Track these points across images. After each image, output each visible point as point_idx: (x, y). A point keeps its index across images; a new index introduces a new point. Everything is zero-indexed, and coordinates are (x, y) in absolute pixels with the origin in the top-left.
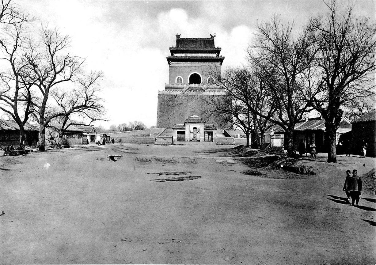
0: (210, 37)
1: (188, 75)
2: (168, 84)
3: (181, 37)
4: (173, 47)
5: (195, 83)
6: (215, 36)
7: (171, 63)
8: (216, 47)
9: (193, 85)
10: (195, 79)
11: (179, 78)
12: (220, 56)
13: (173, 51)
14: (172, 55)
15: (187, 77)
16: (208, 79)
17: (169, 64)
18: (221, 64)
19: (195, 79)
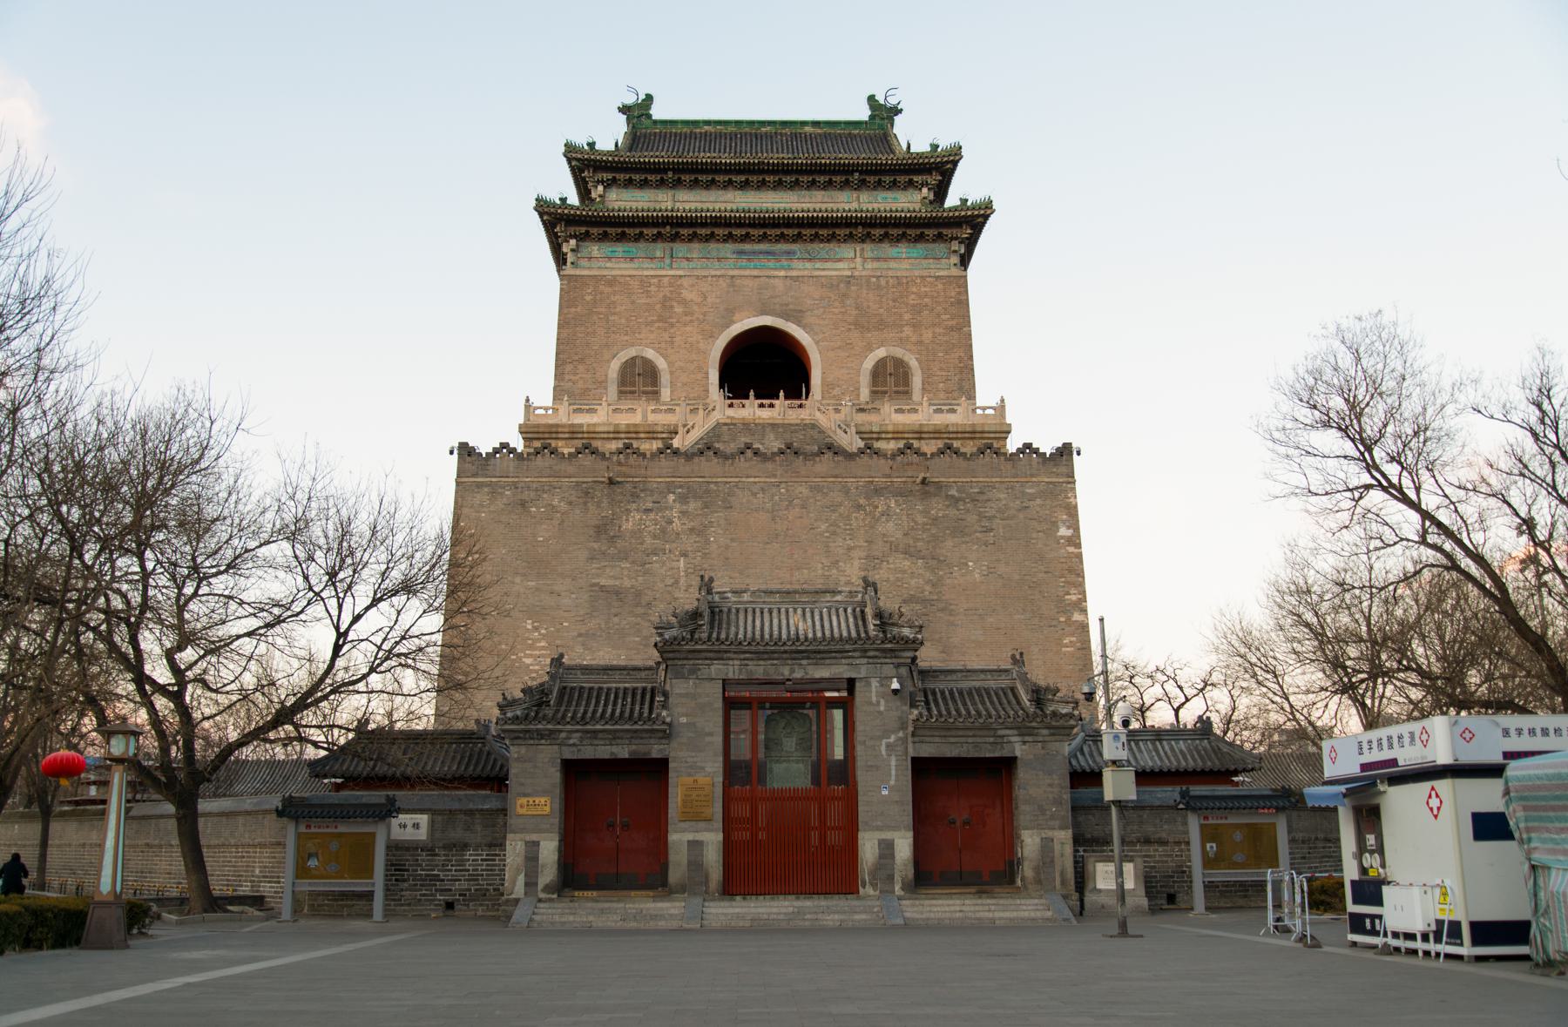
0: (864, 114)
1: (712, 336)
2: (544, 397)
3: (658, 112)
4: (592, 145)
5: (767, 393)
6: (896, 111)
7: (570, 258)
8: (920, 146)
9: (750, 410)
10: (763, 365)
11: (633, 359)
12: (952, 200)
13: (586, 165)
14: (584, 192)
15: (705, 354)
16: (869, 364)
17: (560, 259)
18: (965, 261)
19: (763, 365)
